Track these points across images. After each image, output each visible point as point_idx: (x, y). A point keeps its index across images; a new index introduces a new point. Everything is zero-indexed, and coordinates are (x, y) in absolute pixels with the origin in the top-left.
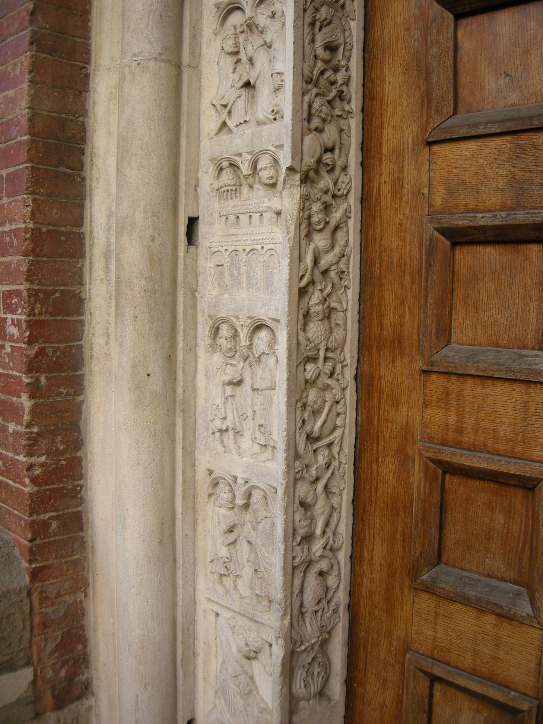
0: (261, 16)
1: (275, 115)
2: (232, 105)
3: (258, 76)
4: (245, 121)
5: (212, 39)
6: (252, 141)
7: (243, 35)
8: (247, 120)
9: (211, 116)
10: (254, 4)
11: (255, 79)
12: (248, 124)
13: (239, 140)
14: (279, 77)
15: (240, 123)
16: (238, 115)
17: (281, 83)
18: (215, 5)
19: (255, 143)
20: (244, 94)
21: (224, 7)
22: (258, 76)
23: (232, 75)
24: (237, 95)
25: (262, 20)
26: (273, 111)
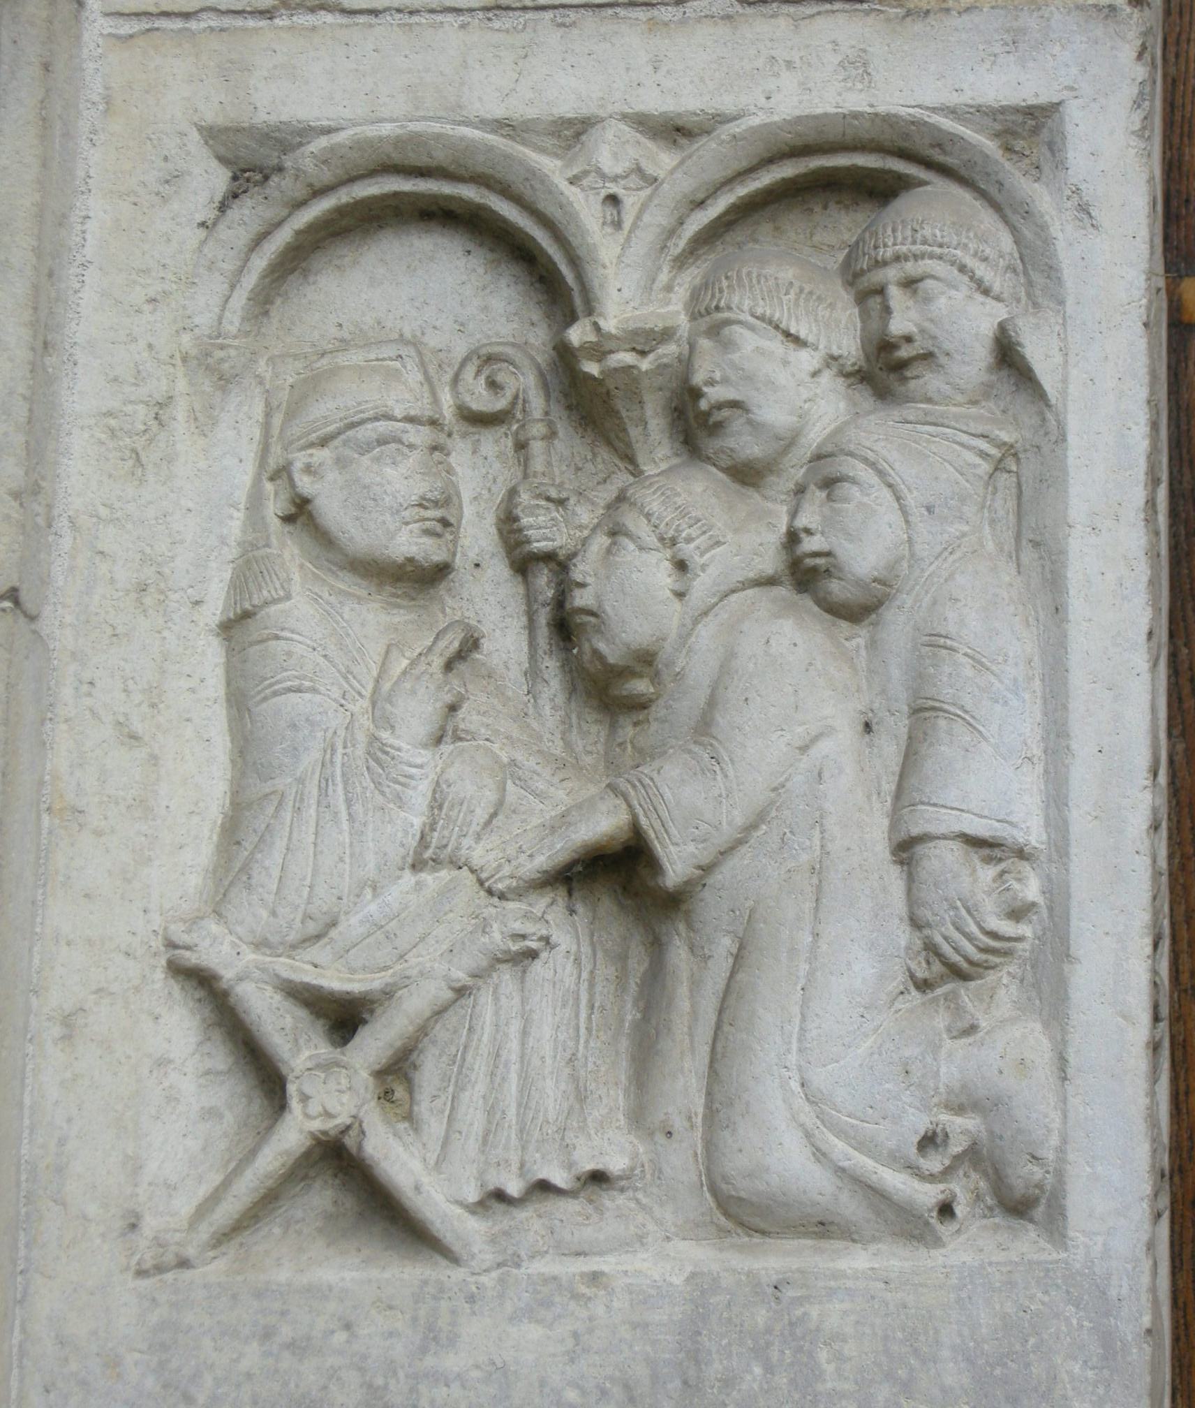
0: (776, 345)
1: (947, 1173)
2: (440, 1012)
3: (752, 827)
4: (598, 1178)
5: (180, 411)
6: (696, 1356)
7: (494, 443)
8: (616, 1164)
9: (162, 1063)
10: (671, 233)
11: (721, 840)
12: (613, 1201)
13: (534, 1332)
14: (988, 873)
15: (544, 1187)
16: (493, 1109)
17: (1007, 927)
18: (211, 134)
19: (727, 1382)
20: (563, 940)
21: (327, 176)
22: (752, 827)
23: (424, 756)
24: (497, 938)
25: (782, 377)
26: (929, 1141)
